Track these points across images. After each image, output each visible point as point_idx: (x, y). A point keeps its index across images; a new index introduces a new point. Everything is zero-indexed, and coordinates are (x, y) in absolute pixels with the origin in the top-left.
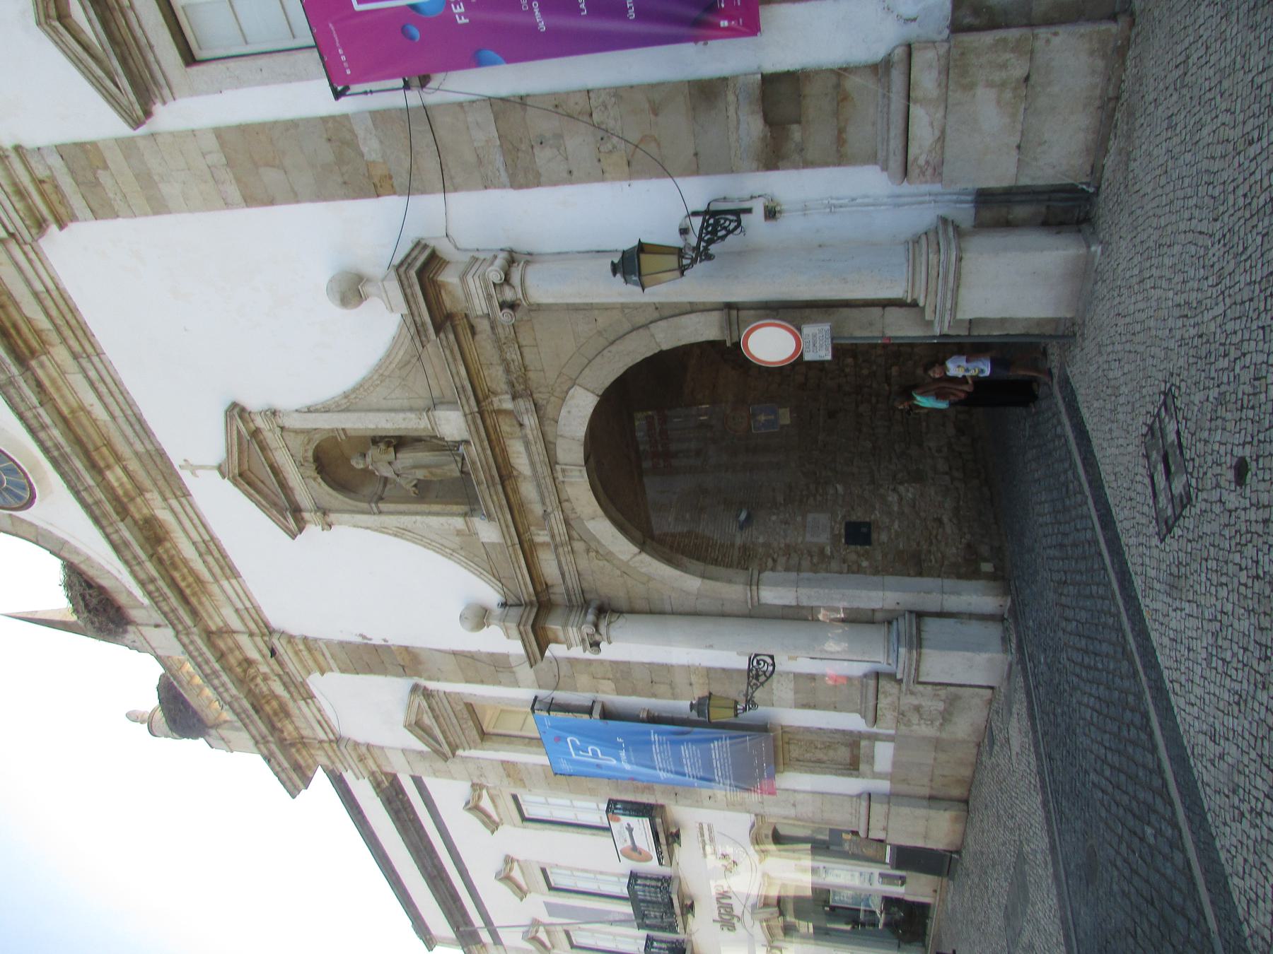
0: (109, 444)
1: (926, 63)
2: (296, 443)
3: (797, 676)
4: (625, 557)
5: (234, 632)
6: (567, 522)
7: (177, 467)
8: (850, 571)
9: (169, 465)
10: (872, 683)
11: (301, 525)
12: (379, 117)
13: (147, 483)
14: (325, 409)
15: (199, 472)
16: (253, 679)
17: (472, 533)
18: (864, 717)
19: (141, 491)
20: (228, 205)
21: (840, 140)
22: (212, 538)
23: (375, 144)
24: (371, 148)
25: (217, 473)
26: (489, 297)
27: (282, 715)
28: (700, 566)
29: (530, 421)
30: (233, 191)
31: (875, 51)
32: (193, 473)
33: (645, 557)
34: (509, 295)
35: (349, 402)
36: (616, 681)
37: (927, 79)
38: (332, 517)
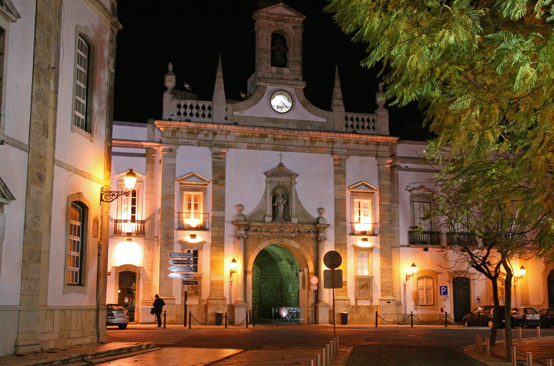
0: (287, 139)
1: (346, 302)
2: (287, 184)
4: (258, 246)
5: (226, 135)
6: (268, 236)
7: (282, 152)
9: (281, 151)
11: (267, 176)
12: (346, 226)
13: (277, 142)
14: (296, 195)
15: (279, 157)
16: (208, 132)
17: (265, 216)
19: (274, 139)
20: (335, 196)
22: (260, 149)
23: (342, 224)
24: (342, 223)
25: (280, 162)
26: (323, 237)
27: (190, 131)
29: (293, 235)
30: (337, 197)
32: (279, 155)
33: (259, 251)
34: (323, 240)
35: (298, 201)
36: (217, 237)
37: (346, 302)
38: (268, 184)
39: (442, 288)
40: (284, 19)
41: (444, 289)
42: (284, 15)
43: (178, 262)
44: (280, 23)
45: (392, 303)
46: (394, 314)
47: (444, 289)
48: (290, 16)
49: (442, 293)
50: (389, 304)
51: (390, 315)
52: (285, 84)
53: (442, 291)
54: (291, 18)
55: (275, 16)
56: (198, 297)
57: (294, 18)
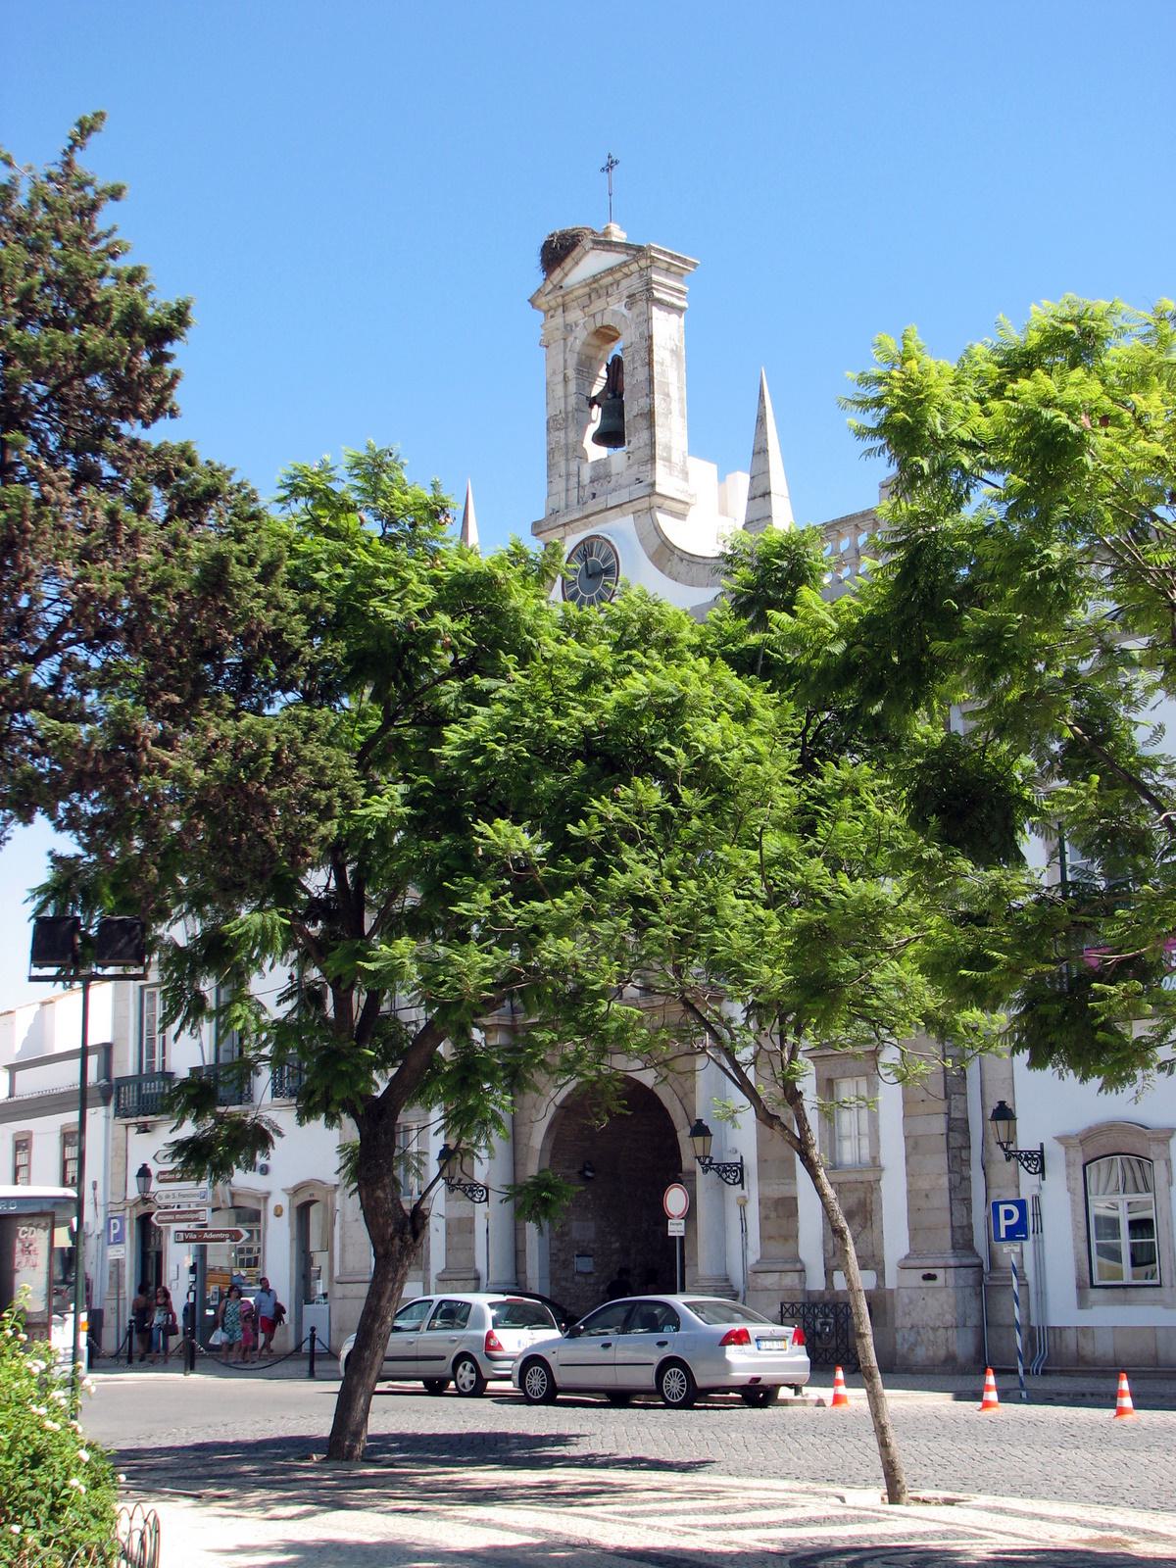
3: (472, 1220)
8: (552, 1255)
10: (472, 1275)
18: (443, 1272)
21: (770, 1238)
28: (549, 1146)
31: (802, 1255)
33: (552, 1109)
39: (1002, 1208)
40: (607, 287)
41: (1009, 1215)
42: (595, 279)
43: (172, 1176)
44: (598, 304)
45: (940, 1281)
46: (946, 1328)
47: (1009, 1215)
48: (611, 271)
49: (1003, 1235)
50: (931, 1283)
51: (935, 1329)
52: (601, 511)
53: (1003, 1223)
54: (618, 275)
55: (581, 292)
56: (421, 1273)
57: (626, 270)
